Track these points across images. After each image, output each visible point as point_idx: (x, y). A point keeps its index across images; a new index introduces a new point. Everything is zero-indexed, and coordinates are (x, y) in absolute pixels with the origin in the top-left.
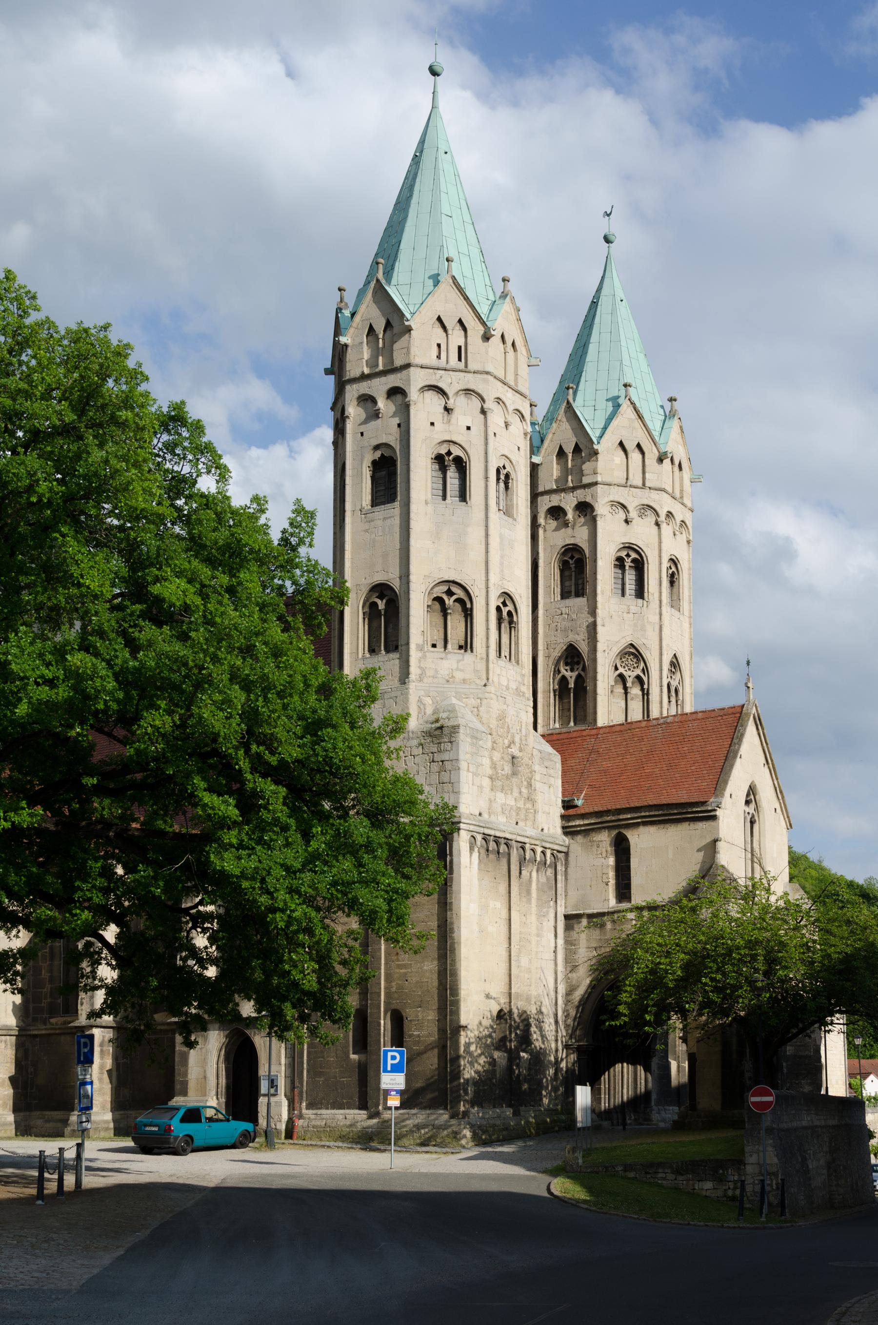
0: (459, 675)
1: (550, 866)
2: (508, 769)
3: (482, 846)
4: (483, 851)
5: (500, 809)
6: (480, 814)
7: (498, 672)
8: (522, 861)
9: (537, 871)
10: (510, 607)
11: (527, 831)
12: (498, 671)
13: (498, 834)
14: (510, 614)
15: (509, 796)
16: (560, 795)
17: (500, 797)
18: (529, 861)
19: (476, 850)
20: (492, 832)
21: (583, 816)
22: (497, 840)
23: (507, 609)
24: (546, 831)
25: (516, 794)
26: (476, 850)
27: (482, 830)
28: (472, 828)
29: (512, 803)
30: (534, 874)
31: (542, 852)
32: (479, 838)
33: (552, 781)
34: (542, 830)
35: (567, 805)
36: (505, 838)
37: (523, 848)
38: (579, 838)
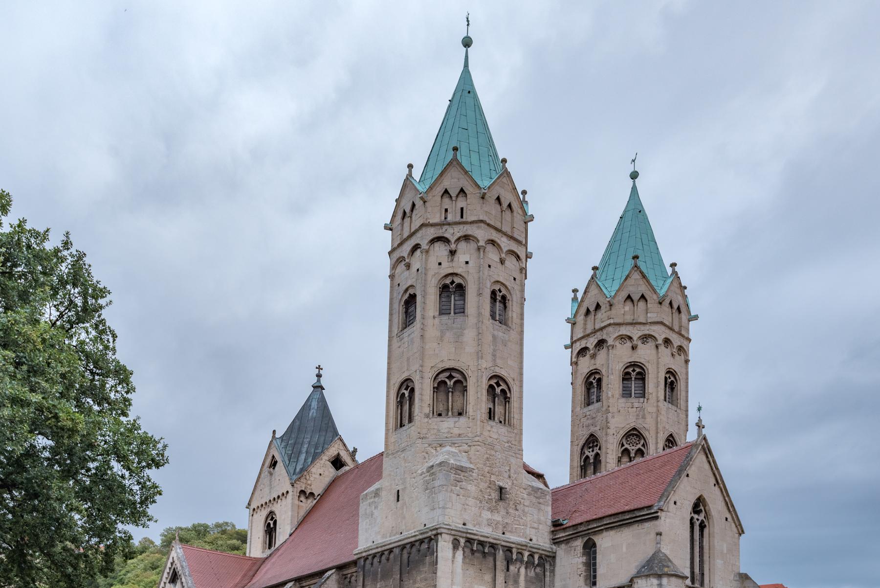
0: (456, 431)
1: (538, 565)
2: (495, 495)
3: (465, 546)
4: (467, 550)
5: (485, 522)
6: (464, 524)
7: (489, 428)
8: (509, 562)
9: (526, 568)
10: (503, 386)
11: (513, 538)
12: (489, 428)
13: (482, 539)
14: (503, 391)
15: (496, 515)
16: (550, 518)
17: (486, 515)
18: (516, 560)
19: (461, 549)
20: (476, 537)
21: (565, 529)
22: (481, 543)
23: (501, 388)
24: (534, 541)
25: (503, 512)
26: (461, 549)
27: (464, 535)
28: (453, 532)
29: (499, 519)
30: (523, 570)
31: (530, 555)
32: (462, 541)
33: (542, 507)
34: (531, 540)
35: (556, 524)
36: (490, 543)
37: (511, 552)
38: (563, 546)
